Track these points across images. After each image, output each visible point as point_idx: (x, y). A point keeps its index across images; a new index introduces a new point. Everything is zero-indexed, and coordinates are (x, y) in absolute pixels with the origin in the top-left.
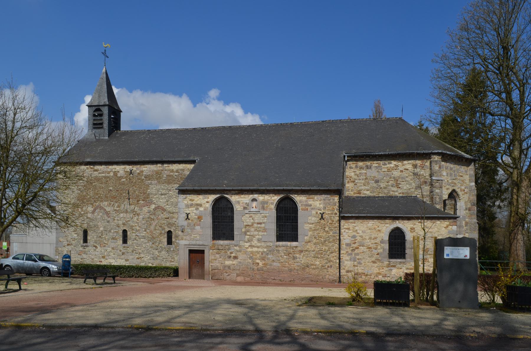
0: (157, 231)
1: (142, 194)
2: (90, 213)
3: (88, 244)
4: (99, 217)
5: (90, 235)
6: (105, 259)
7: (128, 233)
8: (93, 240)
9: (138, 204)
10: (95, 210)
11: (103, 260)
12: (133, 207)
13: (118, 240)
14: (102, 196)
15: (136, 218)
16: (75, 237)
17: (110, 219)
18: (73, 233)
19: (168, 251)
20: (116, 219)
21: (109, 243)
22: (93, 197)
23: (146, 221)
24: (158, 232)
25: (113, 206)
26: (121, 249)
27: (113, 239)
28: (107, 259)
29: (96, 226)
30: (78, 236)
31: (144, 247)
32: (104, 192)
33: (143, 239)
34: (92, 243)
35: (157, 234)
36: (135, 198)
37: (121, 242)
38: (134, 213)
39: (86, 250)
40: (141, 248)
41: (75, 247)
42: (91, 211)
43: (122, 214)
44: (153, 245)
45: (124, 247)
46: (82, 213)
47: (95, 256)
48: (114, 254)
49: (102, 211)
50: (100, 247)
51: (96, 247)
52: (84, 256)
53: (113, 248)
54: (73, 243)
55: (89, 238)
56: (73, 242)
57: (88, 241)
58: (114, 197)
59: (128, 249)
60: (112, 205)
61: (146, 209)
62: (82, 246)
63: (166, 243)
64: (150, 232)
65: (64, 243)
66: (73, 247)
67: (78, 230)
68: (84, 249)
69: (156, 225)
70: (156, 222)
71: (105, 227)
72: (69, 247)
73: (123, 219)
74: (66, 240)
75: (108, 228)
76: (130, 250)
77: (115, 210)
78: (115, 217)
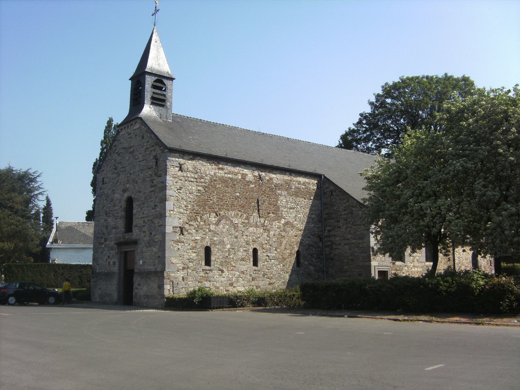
4: (225, 230)
7: (259, 253)
10: (220, 221)
12: (262, 220)
14: (227, 203)
17: (238, 234)
18: (191, 251)
24: (288, 251)
29: (222, 243)
32: (230, 198)
35: (287, 254)
38: (265, 228)
42: (214, 222)
58: (243, 207)
61: (276, 224)
65: (178, 265)
71: (232, 245)
77: (243, 223)
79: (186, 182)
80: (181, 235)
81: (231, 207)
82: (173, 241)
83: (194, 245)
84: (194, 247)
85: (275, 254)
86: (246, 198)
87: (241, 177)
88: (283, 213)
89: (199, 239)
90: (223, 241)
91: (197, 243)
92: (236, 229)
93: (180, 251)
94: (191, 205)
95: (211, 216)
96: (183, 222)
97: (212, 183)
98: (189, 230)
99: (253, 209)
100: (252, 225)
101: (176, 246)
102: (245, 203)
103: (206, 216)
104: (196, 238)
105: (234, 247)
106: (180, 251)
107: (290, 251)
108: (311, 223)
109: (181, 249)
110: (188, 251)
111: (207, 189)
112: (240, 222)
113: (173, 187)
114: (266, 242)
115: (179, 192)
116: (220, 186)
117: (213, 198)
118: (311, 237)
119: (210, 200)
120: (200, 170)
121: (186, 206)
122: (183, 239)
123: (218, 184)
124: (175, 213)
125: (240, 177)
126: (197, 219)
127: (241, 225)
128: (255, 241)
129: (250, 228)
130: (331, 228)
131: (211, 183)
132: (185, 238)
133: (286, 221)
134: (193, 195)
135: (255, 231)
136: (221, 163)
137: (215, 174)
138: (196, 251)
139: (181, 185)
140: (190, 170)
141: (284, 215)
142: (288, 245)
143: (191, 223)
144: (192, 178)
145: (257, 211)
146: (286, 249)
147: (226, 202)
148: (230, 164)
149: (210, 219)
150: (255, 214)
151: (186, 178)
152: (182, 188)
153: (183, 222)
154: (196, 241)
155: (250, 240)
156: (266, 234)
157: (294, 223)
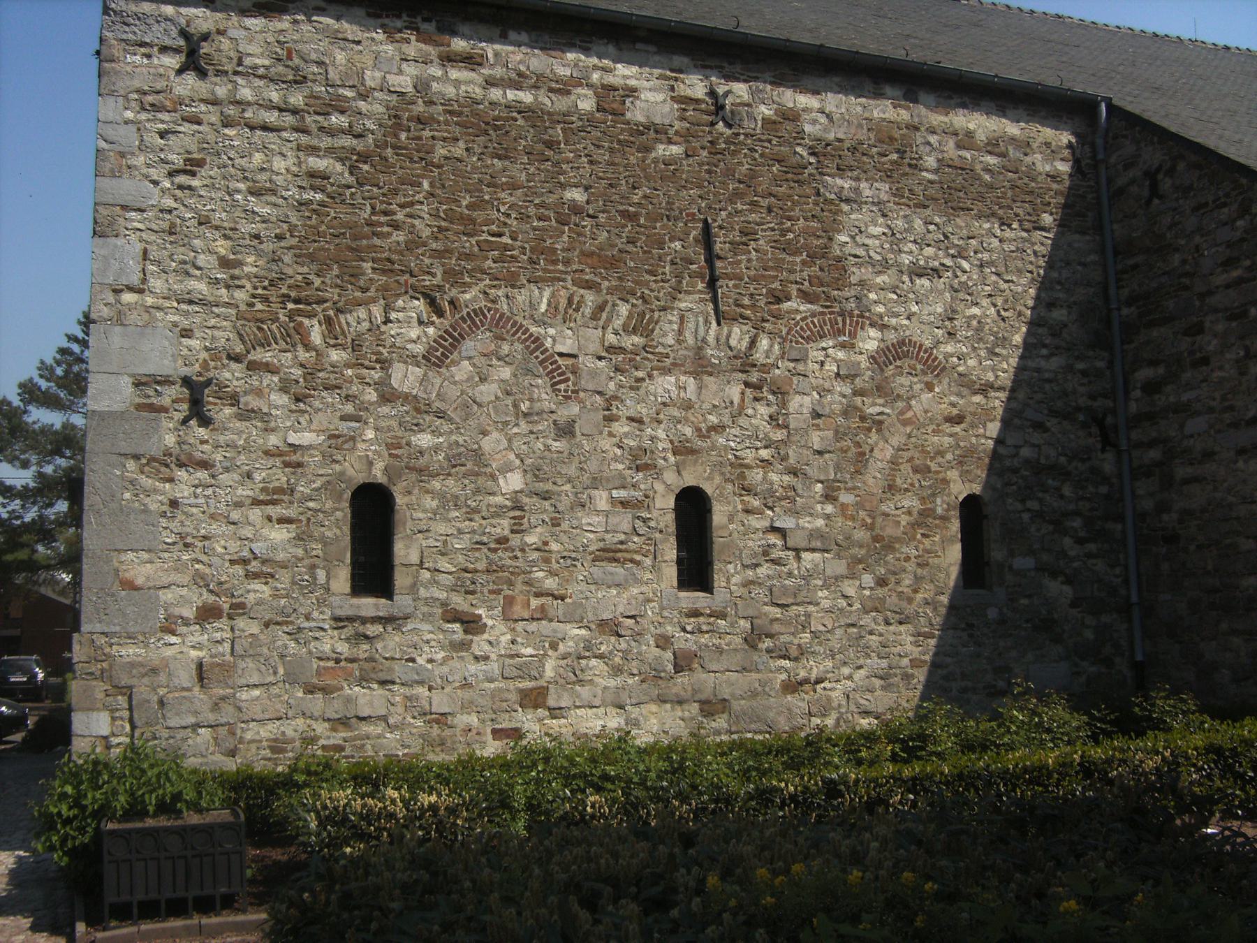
0: (898, 497)
3: (402, 601)
4: (487, 391)
7: (719, 516)
8: (444, 564)
10: (457, 342)
12: (738, 336)
13: (648, 561)
14: (506, 240)
16: (274, 548)
17: (575, 409)
18: (255, 514)
20: (624, 413)
23: (837, 432)
24: (906, 503)
25: (595, 317)
27: (609, 554)
32: (523, 218)
33: (817, 556)
35: (904, 520)
37: (671, 572)
38: (754, 377)
41: (279, 632)
42: (419, 349)
44: (881, 592)
45: (695, 613)
47: (466, 695)
48: (617, 671)
50: (506, 618)
52: (368, 699)
55: (404, 551)
56: (259, 590)
57: (401, 580)
65: (167, 596)
69: (894, 462)
70: (896, 440)
71: (535, 473)
72: (220, 629)
77: (612, 349)
79: (226, 131)
80: (193, 423)
81: (531, 261)
83: (281, 478)
84: (280, 491)
85: (828, 517)
88: (873, 296)
89: (310, 447)
91: (299, 465)
92: (562, 387)
93: (182, 517)
94: (259, 255)
95: (393, 316)
96: (207, 349)
98: (249, 398)
99: (679, 277)
100: (668, 361)
102: (620, 243)
103: (362, 313)
104: (293, 438)
107: (922, 500)
108: (1044, 352)
109: (192, 501)
110: (235, 515)
111: (366, 167)
112: (594, 347)
113: (140, 160)
114: (764, 453)
115: (181, 187)
116: (459, 150)
117: (410, 216)
118: (1051, 423)
119: (386, 229)
120: (320, 63)
121: (224, 263)
122: (206, 447)
124: (150, 300)
125: (587, 104)
126: (299, 329)
127: (602, 364)
128: (692, 452)
129: (660, 380)
130: (1161, 370)
132: (222, 439)
133: (892, 337)
134: (273, 199)
136: (465, 29)
137: (422, 86)
138: (290, 513)
139: (194, 148)
140: (255, 67)
141: (880, 309)
142: (906, 468)
143: (259, 355)
144: (270, 106)
145: (701, 286)
146: (891, 488)
147: (500, 235)
148: (524, 37)
149: (393, 329)
150: (693, 302)
151: (232, 111)
152: (200, 163)
153: (207, 349)
154: (291, 457)
155: (660, 446)
156: (763, 410)
157: (942, 348)
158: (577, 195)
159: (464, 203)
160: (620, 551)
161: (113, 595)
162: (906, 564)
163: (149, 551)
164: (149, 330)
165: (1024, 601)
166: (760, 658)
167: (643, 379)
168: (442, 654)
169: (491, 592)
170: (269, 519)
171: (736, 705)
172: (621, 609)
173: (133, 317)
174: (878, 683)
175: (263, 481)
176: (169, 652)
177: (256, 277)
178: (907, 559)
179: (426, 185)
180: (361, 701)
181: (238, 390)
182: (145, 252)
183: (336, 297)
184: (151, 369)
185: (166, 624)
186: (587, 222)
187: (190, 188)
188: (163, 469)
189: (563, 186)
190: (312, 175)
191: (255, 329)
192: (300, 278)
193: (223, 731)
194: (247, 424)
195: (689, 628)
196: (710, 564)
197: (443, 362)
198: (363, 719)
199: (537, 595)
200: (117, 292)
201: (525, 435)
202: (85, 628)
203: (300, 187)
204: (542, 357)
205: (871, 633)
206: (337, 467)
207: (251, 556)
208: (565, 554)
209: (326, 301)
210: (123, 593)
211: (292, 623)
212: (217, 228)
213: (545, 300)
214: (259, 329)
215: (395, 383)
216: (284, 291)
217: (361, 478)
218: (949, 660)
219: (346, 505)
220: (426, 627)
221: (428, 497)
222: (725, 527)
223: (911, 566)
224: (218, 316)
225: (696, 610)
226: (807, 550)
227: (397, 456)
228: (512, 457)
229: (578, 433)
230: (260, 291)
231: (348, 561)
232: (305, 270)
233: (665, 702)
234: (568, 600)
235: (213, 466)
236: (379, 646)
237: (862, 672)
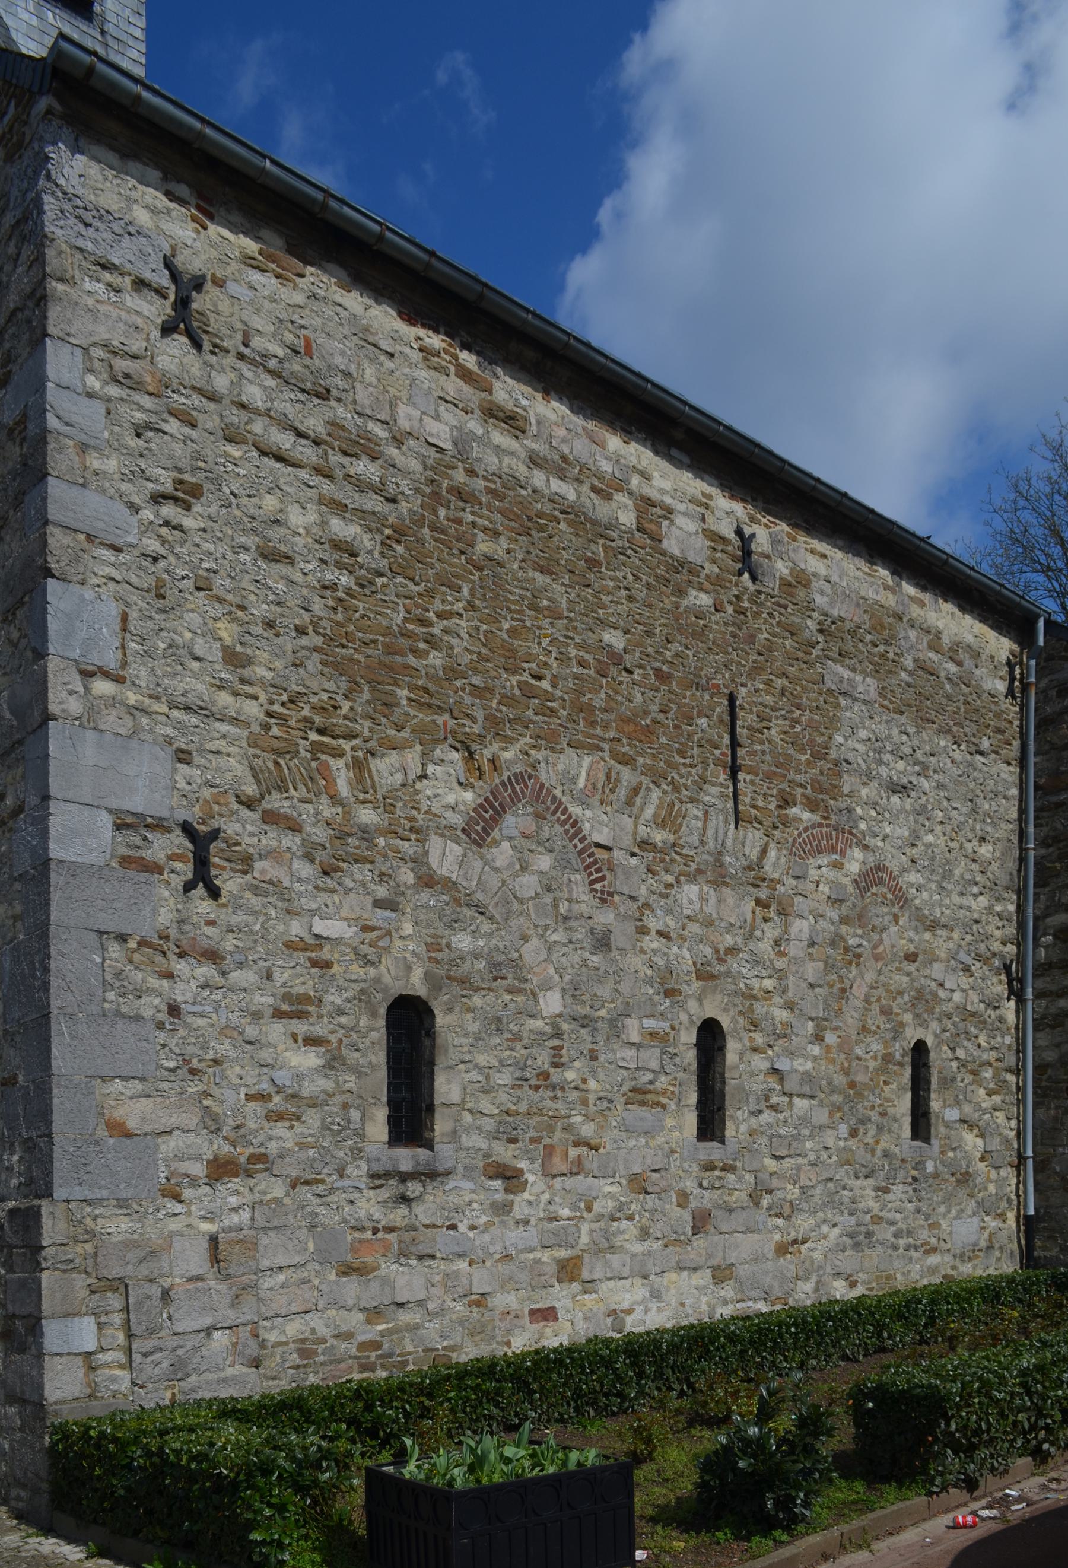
1: (802, 751)
2: (447, 832)
4: (528, 885)
5: (453, 1056)
6: (576, 1286)
8: (486, 1105)
9: (786, 822)
11: (560, 1297)
12: (754, 837)
14: (545, 685)
15: (771, 931)
16: (299, 1077)
18: (276, 1031)
19: (915, 1179)
20: (653, 923)
21: (607, 1140)
22: (477, 680)
25: (629, 803)
26: (690, 1185)
28: (589, 1285)
30: (334, 1063)
31: (812, 1157)
32: (563, 659)
34: (479, 1141)
35: (872, 1064)
36: (769, 776)
39: (423, 1213)
40: (799, 1168)
42: (456, 820)
43: (695, 888)
44: (852, 1143)
45: (709, 1167)
46: (367, 816)
47: (503, 1269)
48: (644, 1234)
49: (552, 830)
51: (511, 1178)
53: (639, 1185)
54: (273, 1148)
57: (441, 1126)
59: (731, 1177)
60: (622, 792)
61: (819, 868)
62: (378, 1178)
63: (907, 1132)
64: (840, 1047)
65: (169, 1146)
66: (278, 1190)
67: (334, 999)
68: (403, 1210)
71: (573, 992)
73: (694, 928)
74: (192, 1120)
75: (596, 1002)
76: (739, 1186)
78: (646, 905)
82: (122, 938)
85: (815, 1059)
86: (657, 671)
87: (632, 515)
89: (338, 941)
90: (516, 964)
91: (328, 965)
92: (598, 886)
97: (442, 512)
100: (694, 866)
101: (154, 982)
103: (393, 757)
104: (320, 927)
105: (585, 1010)
106: (182, 1032)
110: (251, 1032)
111: (400, 549)
112: (627, 841)
117: (446, 631)
119: (422, 645)
123: (485, 530)
125: (627, 518)
126: (325, 773)
127: (634, 861)
128: (712, 977)
129: (687, 888)
131: (435, 512)
135: (710, 908)
142: (875, 1008)
143: (275, 802)
146: (864, 1030)
147: (539, 678)
155: (685, 968)
158: (614, 639)
159: (506, 626)
160: (650, 1092)
161: (97, 1143)
162: (872, 1113)
163: (143, 1079)
164: (134, 744)
165: (951, 1154)
166: (761, 1216)
167: (672, 885)
168: (484, 1219)
169: (533, 1140)
170: (294, 1037)
171: (743, 1271)
172: (649, 1162)
173: (110, 720)
174: (848, 1241)
175: (284, 985)
176: (174, 1225)
177: (273, 686)
178: (873, 1108)
179: (465, 591)
180: (401, 1281)
181: (251, 850)
182: (125, 618)
183: (367, 733)
184: (137, 803)
185: (167, 1187)
186: (624, 677)
187: (178, 527)
188: (159, 958)
189: (604, 624)
190: (337, 545)
191: (271, 765)
192: (325, 696)
193: (244, 1333)
194: (265, 900)
195: (705, 1183)
196: (722, 1108)
197: (484, 840)
198: (401, 1305)
199: (576, 1144)
200: (87, 675)
201: (564, 945)
202: (59, 1193)
203: (323, 561)
204: (580, 846)
205: (844, 1188)
206: (372, 971)
207: (272, 1090)
208: (602, 1094)
209: (355, 737)
210: (111, 1141)
211: (322, 1181)
212: (221, 601)
213: (584, 774)
214: (276, 763)
215: (434, 861)
216: (306, 712)
217: (398, 988)
218: (898, 1216)
219: (382, 1022)
220: (468, 1185)
221: (469, 1016)
222: (736, 1067)
223: (874, 1116)
224: (224, 736)
225: (712, 1162)
226: (799, 1096)
227: (437, 961)
228: (552, 971)
229: (613, 947)
230: (277, 708)
231: (385, 1099)
232: (331, 686)
233: (683, 1269)
234: (601, 1151)
235: (223, 958)
236: (419, 1209)
237: (836, 1231)
